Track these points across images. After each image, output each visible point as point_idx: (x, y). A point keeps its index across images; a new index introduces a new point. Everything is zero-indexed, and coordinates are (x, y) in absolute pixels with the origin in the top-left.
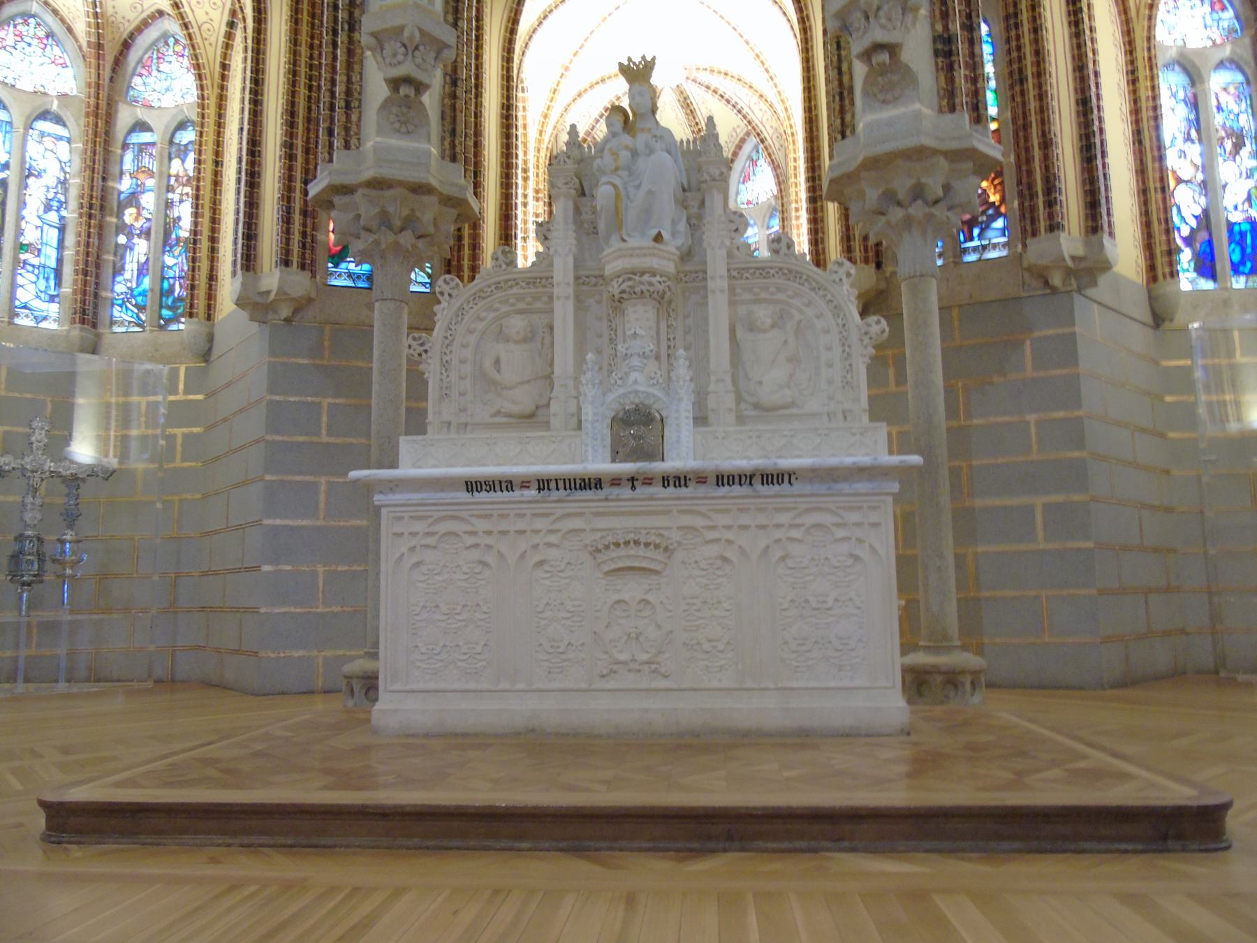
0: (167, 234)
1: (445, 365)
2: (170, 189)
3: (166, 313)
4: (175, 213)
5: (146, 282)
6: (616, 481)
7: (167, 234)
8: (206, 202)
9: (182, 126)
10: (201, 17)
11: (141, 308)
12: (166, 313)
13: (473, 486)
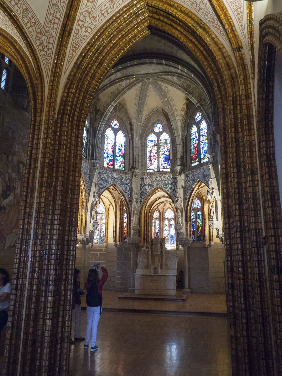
0: (101, 230)
1: (139, 261)
2: (101, 224)
3: (101, 241)
4: (102, 227)
5: (98, 237)
6: (153, 275)
7: (101, 230)
8: (106, 228)
9: (103, 216)
10: (106, 204)
11: (98, 240)
12: (101, 241)
13: (143, 275)
